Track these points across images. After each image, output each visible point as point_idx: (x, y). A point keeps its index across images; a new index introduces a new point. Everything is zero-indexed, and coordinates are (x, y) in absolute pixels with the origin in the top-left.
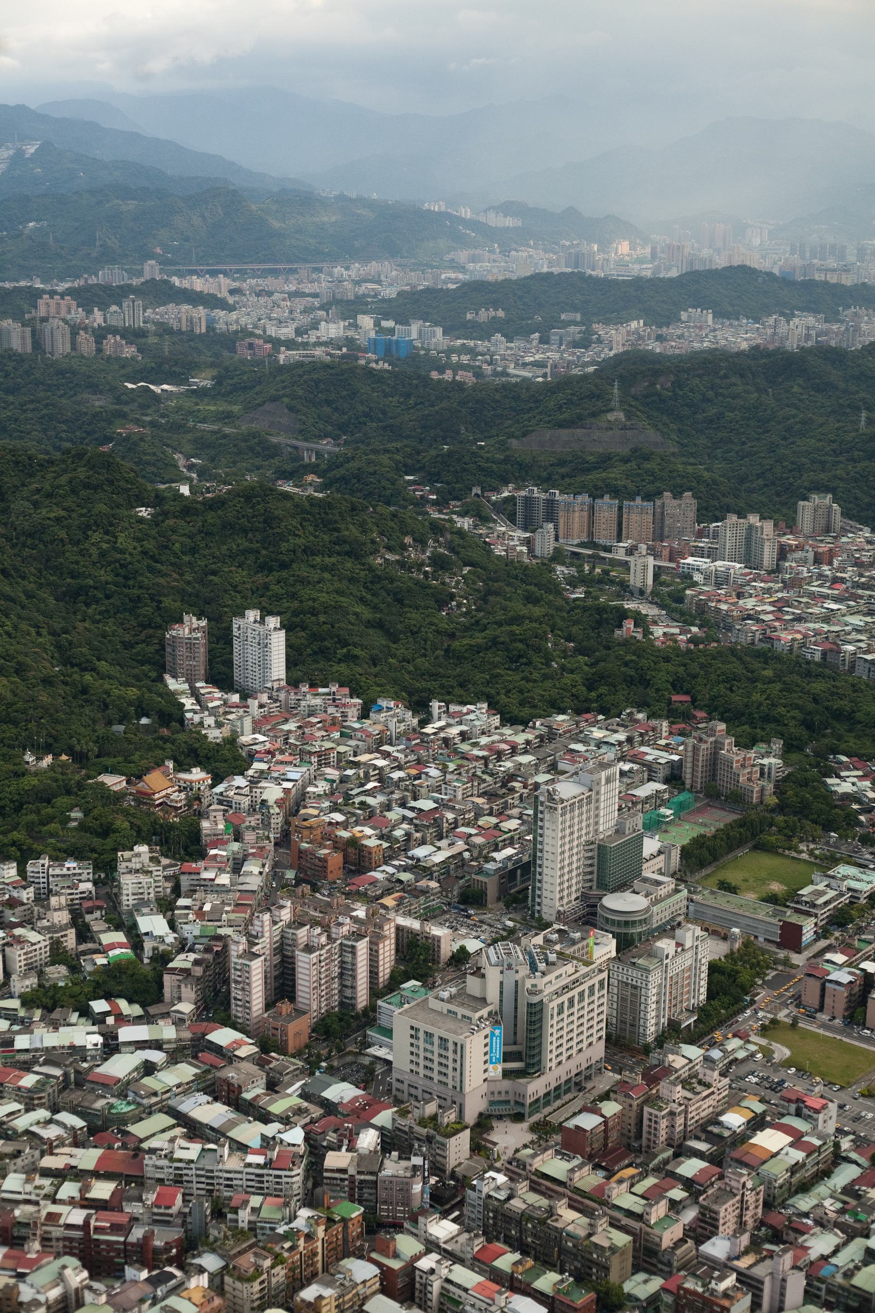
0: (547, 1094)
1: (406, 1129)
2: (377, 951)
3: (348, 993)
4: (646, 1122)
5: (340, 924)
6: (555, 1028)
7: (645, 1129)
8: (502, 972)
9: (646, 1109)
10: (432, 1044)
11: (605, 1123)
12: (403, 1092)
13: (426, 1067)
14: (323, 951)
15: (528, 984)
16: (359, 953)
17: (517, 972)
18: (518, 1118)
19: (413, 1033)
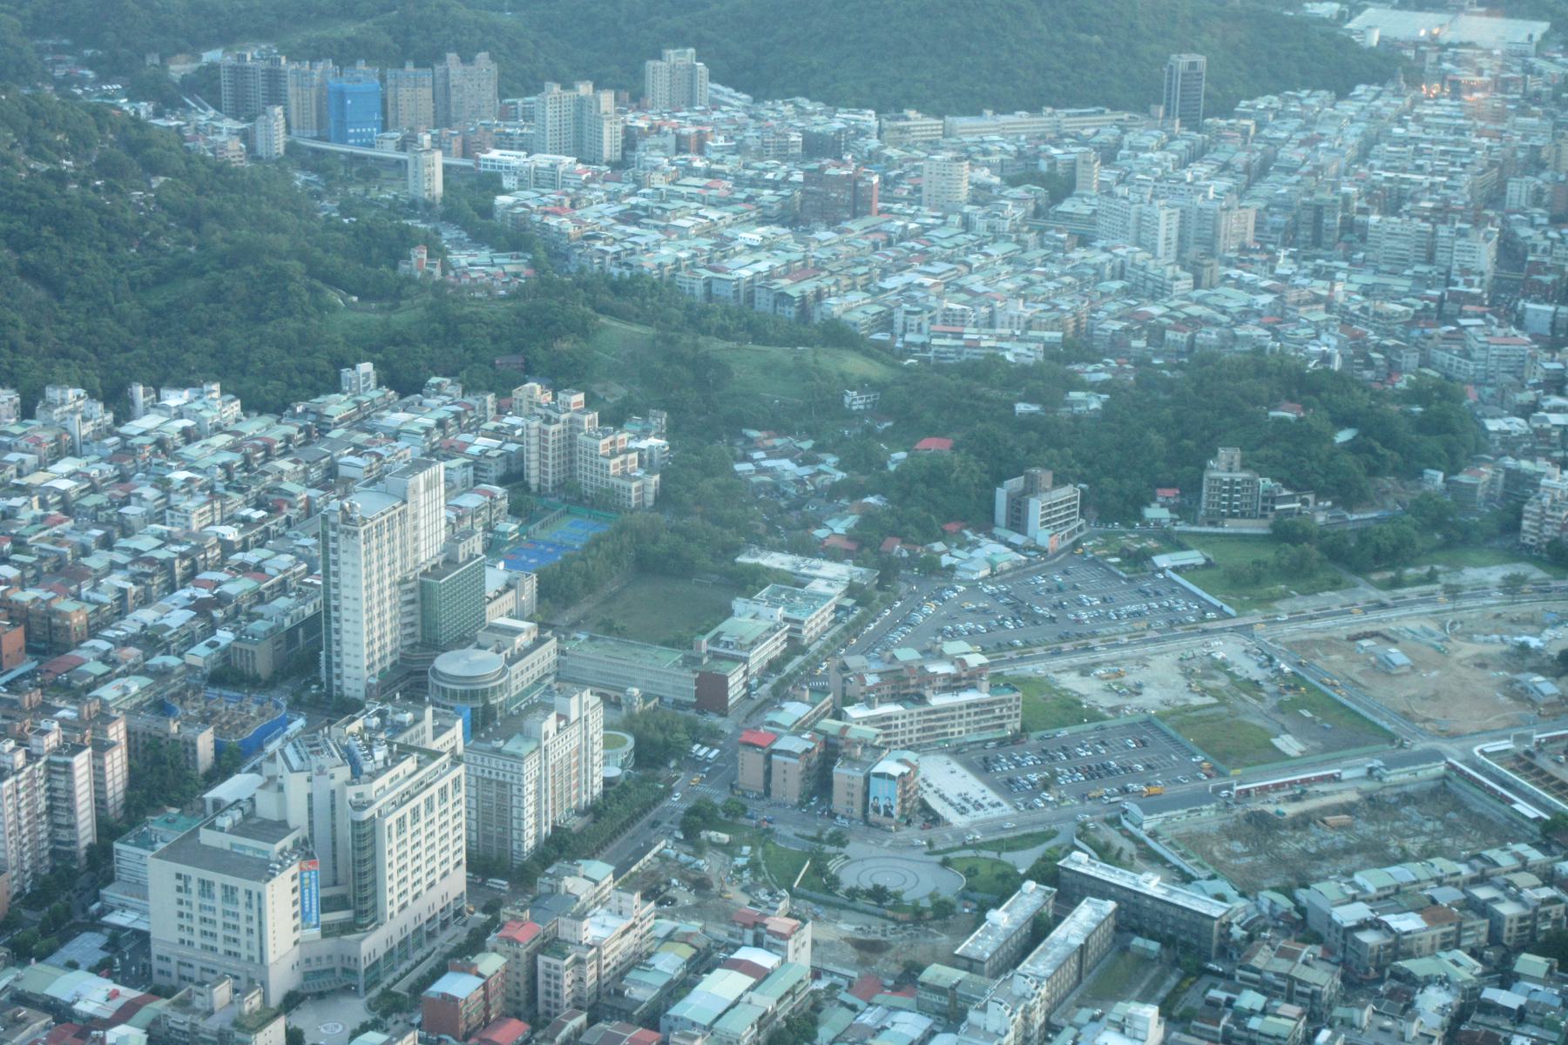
0: (390, 953)
1: (186, 1028)
2: (102, 768)
3: (63, 834)
4: (541, 978)
5: (44, 733)
6: (396, 855)
7: (541, 987)
8: (309, 780)
9: (541, 959)
10: (212, 896)
11: (485, 986)
12: (169, 975)
13: (204, 933)
14: (22, 776)
15: (351, 793)
16: (78, 773)
17: (332, 777)
18: (348, 990)
19: (181, 883)
